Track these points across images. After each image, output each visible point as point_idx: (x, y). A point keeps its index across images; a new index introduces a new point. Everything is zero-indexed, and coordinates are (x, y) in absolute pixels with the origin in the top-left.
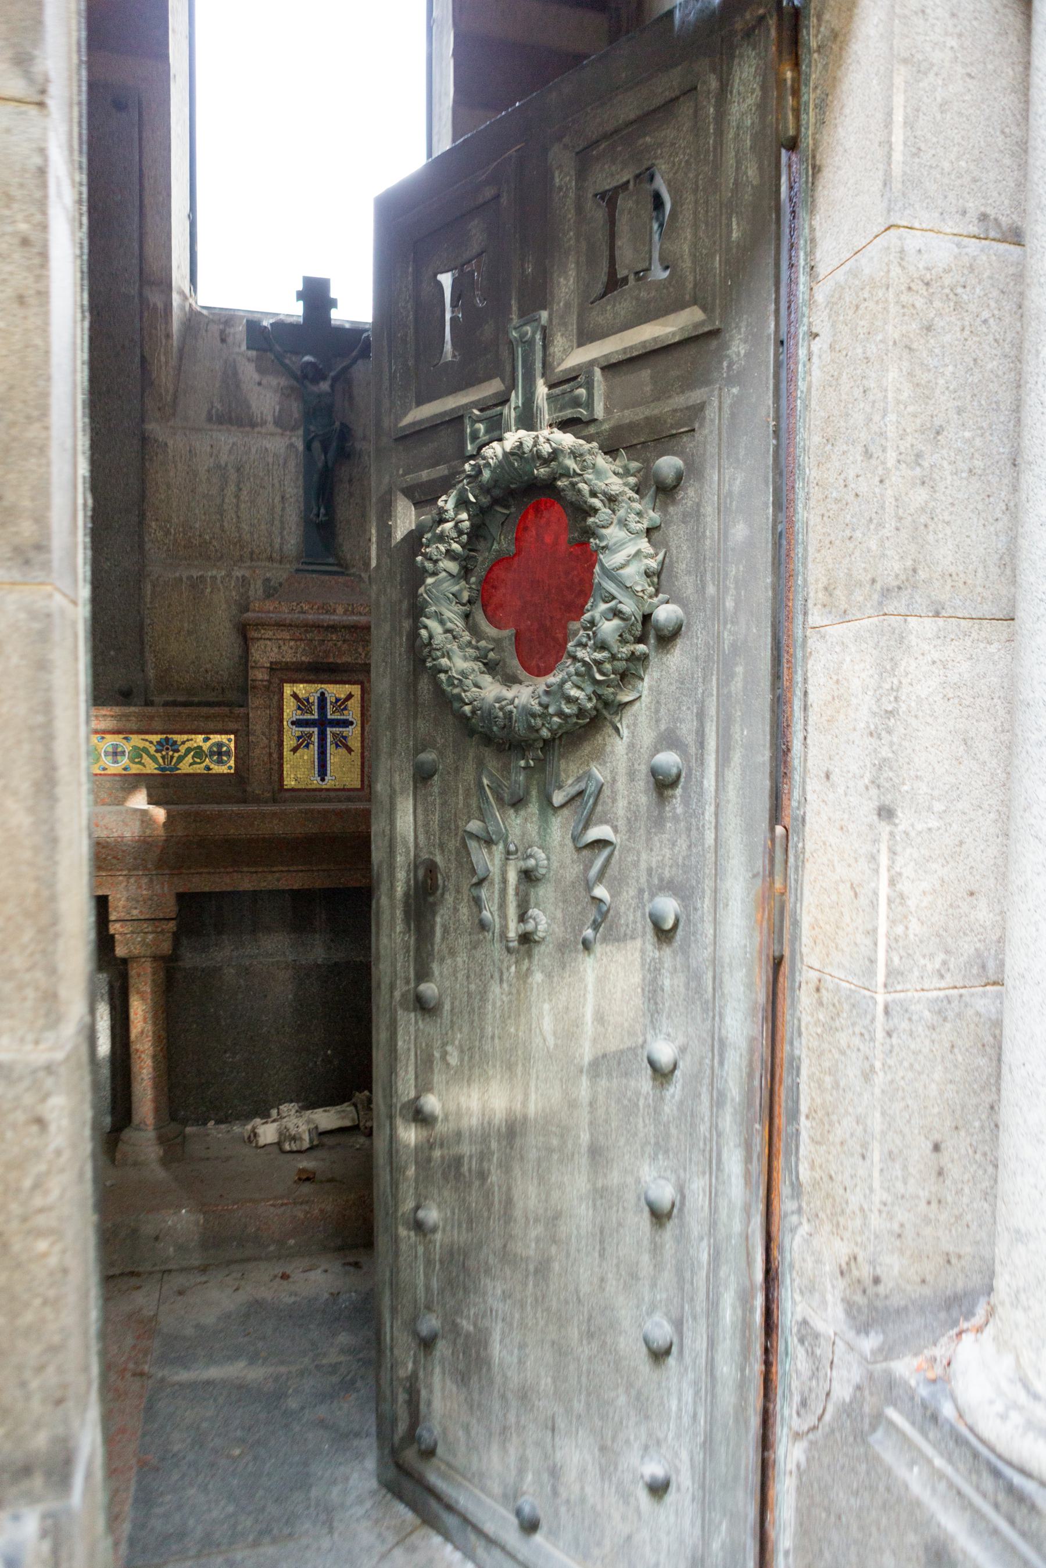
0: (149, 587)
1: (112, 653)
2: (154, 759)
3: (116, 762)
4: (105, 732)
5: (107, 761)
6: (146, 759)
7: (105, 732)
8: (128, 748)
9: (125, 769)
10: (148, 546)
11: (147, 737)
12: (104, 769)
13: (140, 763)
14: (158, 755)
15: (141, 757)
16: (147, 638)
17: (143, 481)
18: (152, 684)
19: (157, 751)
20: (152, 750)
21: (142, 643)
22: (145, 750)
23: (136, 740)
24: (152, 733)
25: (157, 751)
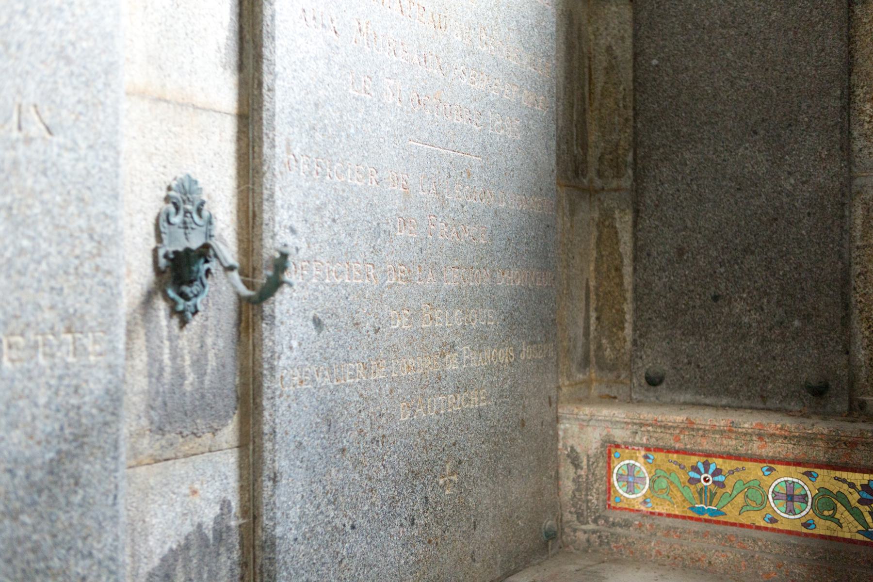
0: (859, 212)
1: (796, 323)
2: (857, 515)
3: (791, 511)
4: (773, 461)
5: (778, 509)
6: (842, 513)
7: (773, 461)
8: (810, 489)
9: (806, 525)
10: (857, 145)
11: (844, 475)
12: (773, 520)
13: (832, 518)
14: (865, 509)
15: (835, 509)
16: (856, 297)
17: (850, 40)
18: (863, 374)
19: (862, 501)
20: (854, 498)
21: (847, 306)
22: (841, 497)
23: (826, 478)
24: (854, 470)
25: (862, 501)
